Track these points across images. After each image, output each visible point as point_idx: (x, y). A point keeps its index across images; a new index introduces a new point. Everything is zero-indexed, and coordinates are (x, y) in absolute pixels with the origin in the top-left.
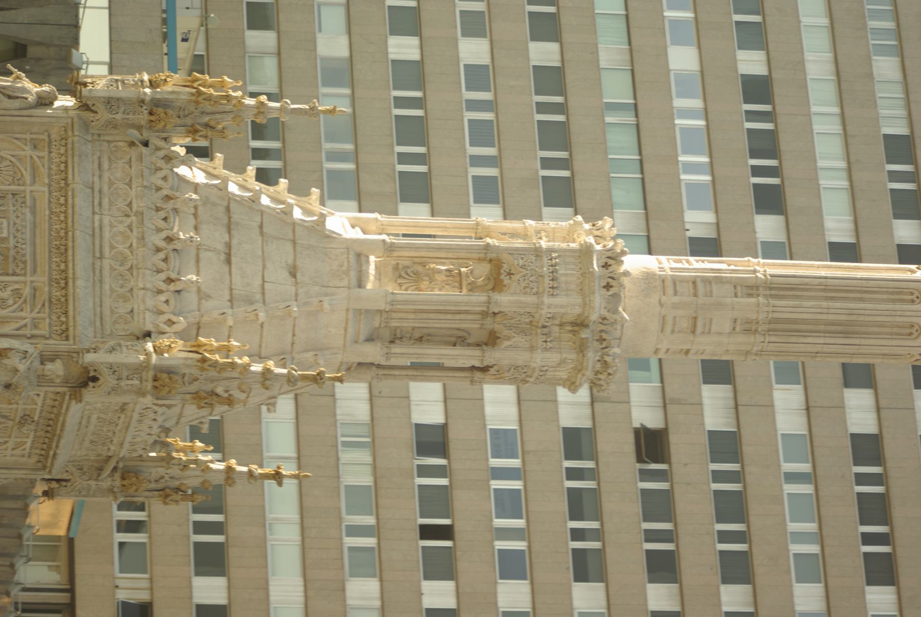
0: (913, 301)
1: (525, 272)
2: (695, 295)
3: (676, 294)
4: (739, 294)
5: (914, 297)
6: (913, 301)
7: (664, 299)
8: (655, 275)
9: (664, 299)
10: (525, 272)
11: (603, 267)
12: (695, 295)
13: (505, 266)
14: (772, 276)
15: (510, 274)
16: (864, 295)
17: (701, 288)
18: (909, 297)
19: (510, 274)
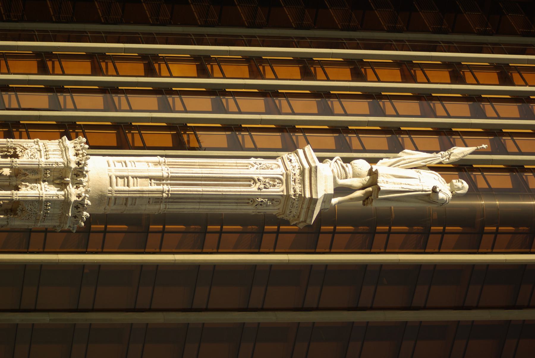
0: (248, 203)
1: (31, 212)
2: (126, 204)
3: (115, 204)
4: (151, 202)
5: (250, 201)
6: (248, 203)
7: (108, 207)
8: (106, 196)
9: (108, 207)
10: (31, 212)
11: (75, 207)
12: (128, 186)
13: (20, 206)
14: (171, 194)
15: (22, 210)
16: (221, 201)
17: (129, 202)
18: (247, 201)
19: (22, 210)
